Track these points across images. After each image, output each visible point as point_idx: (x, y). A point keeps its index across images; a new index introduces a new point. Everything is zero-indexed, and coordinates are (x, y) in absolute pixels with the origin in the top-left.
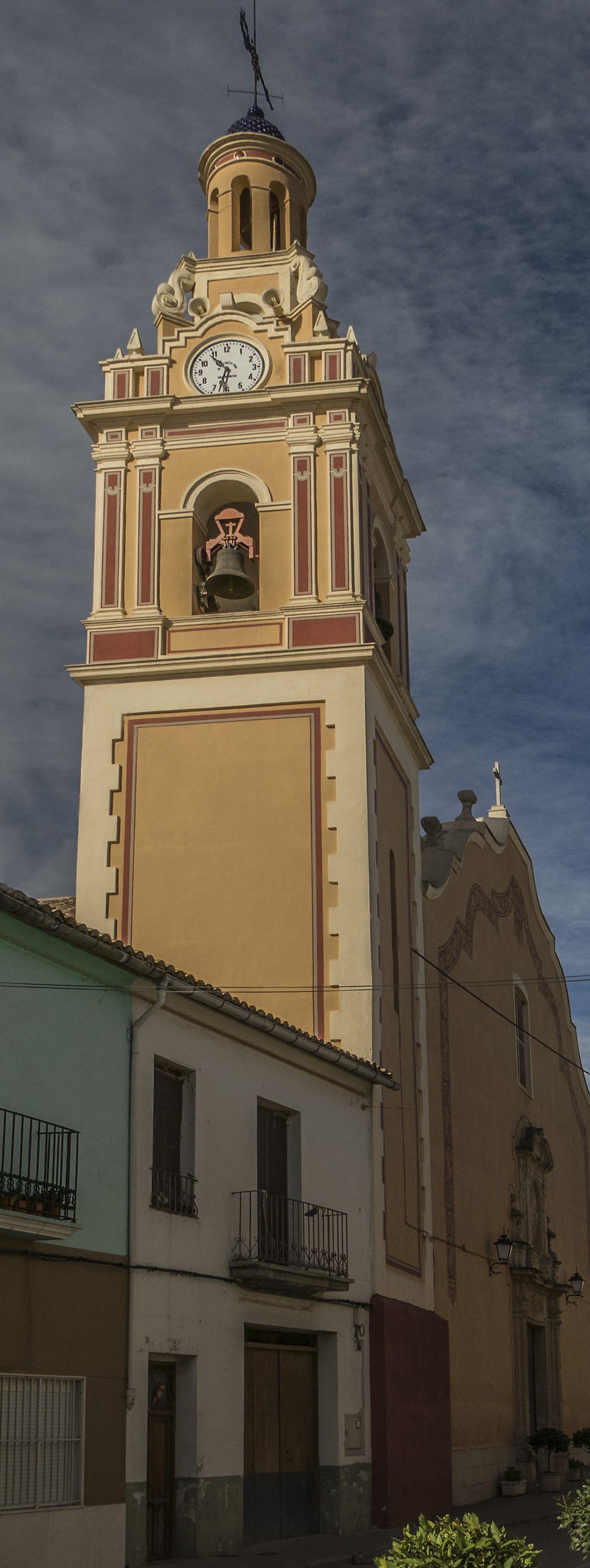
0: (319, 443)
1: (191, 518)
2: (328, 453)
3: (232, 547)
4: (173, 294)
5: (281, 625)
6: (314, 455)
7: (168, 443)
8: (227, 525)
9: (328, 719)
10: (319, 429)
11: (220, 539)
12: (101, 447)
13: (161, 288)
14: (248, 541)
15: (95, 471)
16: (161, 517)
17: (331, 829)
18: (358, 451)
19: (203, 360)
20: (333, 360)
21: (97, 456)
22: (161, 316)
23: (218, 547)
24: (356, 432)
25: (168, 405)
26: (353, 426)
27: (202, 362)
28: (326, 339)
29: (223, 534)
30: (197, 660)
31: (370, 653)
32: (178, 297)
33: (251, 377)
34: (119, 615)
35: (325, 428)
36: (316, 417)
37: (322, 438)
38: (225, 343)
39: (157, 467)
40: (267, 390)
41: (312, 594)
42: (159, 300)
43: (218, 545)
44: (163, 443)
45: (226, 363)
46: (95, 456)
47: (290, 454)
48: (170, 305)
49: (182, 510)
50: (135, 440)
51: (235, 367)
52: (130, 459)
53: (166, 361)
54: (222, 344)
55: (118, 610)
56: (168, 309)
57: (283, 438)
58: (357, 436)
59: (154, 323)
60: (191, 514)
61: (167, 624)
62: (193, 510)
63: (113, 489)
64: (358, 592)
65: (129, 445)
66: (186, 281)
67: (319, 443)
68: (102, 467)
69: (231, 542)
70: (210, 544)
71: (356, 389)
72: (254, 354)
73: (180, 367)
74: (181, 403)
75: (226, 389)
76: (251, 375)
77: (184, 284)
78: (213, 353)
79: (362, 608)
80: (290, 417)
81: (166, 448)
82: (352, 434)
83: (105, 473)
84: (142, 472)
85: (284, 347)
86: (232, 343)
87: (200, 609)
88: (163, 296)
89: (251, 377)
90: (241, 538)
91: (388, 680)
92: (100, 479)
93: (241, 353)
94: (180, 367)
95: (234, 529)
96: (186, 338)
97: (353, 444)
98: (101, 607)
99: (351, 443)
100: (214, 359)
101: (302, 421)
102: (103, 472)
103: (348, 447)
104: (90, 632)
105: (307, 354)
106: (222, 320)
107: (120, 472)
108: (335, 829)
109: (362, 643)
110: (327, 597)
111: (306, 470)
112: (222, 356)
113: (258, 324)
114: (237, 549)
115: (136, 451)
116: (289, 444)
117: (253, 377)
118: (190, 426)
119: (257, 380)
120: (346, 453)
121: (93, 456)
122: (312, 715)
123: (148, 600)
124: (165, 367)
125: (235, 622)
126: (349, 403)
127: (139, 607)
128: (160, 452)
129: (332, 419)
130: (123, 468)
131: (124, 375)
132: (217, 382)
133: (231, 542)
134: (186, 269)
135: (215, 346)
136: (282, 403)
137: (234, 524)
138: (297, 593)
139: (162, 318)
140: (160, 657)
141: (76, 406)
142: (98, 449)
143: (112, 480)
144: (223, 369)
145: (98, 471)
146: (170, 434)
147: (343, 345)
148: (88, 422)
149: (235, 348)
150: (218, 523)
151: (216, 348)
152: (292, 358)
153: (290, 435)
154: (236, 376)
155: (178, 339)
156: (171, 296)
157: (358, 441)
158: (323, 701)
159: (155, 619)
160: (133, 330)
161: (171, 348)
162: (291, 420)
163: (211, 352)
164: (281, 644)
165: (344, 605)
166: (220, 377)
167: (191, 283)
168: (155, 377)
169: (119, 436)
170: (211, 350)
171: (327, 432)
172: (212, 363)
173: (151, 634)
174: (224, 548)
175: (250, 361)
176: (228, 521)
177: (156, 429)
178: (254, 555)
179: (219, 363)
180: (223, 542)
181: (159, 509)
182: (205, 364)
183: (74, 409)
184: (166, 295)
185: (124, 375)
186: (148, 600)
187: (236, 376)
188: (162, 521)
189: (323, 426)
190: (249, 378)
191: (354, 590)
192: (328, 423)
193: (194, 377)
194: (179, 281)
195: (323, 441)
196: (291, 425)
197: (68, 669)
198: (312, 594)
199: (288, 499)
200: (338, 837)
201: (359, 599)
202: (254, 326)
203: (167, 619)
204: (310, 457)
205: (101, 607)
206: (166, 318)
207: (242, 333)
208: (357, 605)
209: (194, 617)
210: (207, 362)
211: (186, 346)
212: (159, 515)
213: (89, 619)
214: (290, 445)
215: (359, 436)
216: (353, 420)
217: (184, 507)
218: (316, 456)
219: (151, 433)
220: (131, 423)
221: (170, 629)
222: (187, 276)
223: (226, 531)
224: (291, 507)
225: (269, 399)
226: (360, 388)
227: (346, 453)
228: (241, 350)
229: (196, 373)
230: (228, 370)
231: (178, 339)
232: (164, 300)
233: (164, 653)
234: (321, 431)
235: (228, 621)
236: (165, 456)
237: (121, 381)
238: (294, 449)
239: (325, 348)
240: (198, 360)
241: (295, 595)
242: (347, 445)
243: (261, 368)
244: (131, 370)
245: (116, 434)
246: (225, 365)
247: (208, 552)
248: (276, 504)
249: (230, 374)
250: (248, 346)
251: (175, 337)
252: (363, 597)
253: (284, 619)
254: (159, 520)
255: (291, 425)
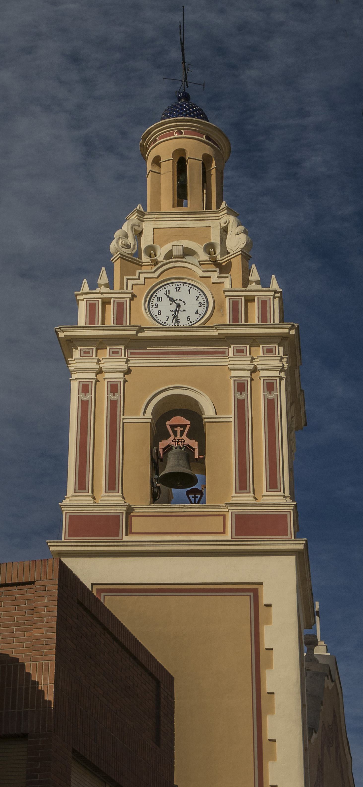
0: (255, 370)
1: (150, 423)
2: (262, 379)
3: (181, 448)
4: (127, 238)
5: (224, 516)
6: (250, 380)
7: (131, 361)
8: (175, 429)
9: (265, 599)
10: (254, 359)
11: (169, 441)
12: (76, 361)
13: (118, 234)
14: (194, 444)
15: (70, 380)
16: (125, 421)
17: (269, 693)
18: (286, 379)
19: (158, 296)
20: (264, 304)
21: (73, 368)
22: (119, 255)
23: (168, 448)
24: (284, 363)
25: (134, 333)
26: (282, 358)
27: (158, 298)
28: (260, 287)
29: (173, 437)
30: (158, 543)
31: (302, 547)
32: (131, 241)
33: (197, 312)
34: (89, 500)
35: (260, 358)
36: (251, 348)
37: (257, 366)
38: (177, 284)
39: (122, 380)
40: (216, 327)
41: (250, 493)
42: (117, 243)
43: (169, 446)
44: (127, 361)
45: (177, 300)
46: (71, 368)
47: (231, 377)
48: (126, 247)
49: (141, 416)
50: (105, 358)
51: (185, 304)
52: (100, 372)
53: (130, 295)
54: (174, 284)
55: (89, 496)
56: (124, 250)
57: (226, 364)
58: (286, 367)
59: (111, 260)
60: (150, 420)
61: (130, 510)
62: (152, 417)
63: (85, 395)
64: (287, 493)
65: (99, 360)
66: (136, 228)
67: (255, 370)
68: (77, 377)
69: (180, 443)
70: (163, 444)
71: (286, 331)
72: (200, 295)
73: (141, 301)
74: (144, 331)
75: (177, 321)
76: (197, 311)
77: (135, 230)
78: (166, 291)
79: (292, 508)
80: (230, 347)
81: (129, 365)
82: (282, 365)
83: (79, 382)
84: (110, 383)
85: (225, 291)
86: (182, 284)
87: (158, 499)
88: (121, 239)
89: (197, 312)
90: (188, 441)
91: (307, 564)
92: (75, 387)
93: (189, 293)
94: (141, 301)
95: (182, 433)
96: (145, 278)
97: (281, 372)
98: (75, 493)
99: (281, 371)
100: (168, 296)
101: (240, 351)
102: (78, 381)
103: (278, 375)
104: (66, 513)
105: (243, 298)
106: (174, 265)
107: (92, 382)
108: (273, 693)
109: (293, 538)
110: (263, 496)
111: (244, 391)
112: (174, 294)
113: (204, 271)
114: (184, 450)
115: (105, 365)
116: (230, 369)
117: (199, 313)
118: (148, 349)
119: (202, 315)
120: (277, 380)
121: (69, 368)
122: (252, 594)
123: (114, 489)
124: (128, 300)
125: (186, 512)
126: (279, 340)
127: (107, 494)
128: (125, 368)
129: (265, 351)
130: (94, 379)
131: (95, 304)
132: (171, 315)
133: (180, 443)
134: (137, 218)
135: (168, 286)
136: (226, 337)
137: (182, 429)
138: (238, 491)
139: (120, 257)
140: (125, 538)
141: (60, 328)
142: (74, 362)
143: (85, 388)
144: (174, 306)
145: (74, 379)
146: (132, 354)
147: (272, 293)
148: (67, 340)
149: (184, 288)
150: (168, 427)
151: (168, 288)
152: (231, 300)
153: (231, 363)
154: (185, 311)
155: (139, 279)
156: (125, 239)
157: (286, 370)
158: (262, 584)
159: (121, 505)
160: (101, 269)
161: (133, 285)
162: (231, 350)
163: (165, 290)
164: (224, 532)
165: (278, 504)
166: (172, 311)
167: (140, 229)
168: (120, 308)
169: (91, 353)
170: (165, 288)
171: (261, 362)
172: (166, 300)
173: (117, 518)
174: (173, 448)
175: (197, 300)
176: (176, 426)
177: (121, 349)
178: (199, 454)
179: (172, 300)
180: (173, 443)
181: (123, 415)
182: (160, 299)
183: (57, 330)
184: (123, 239)
185: (95, 304)
186: (114, 489)
187: (185, 311)
188: (125, 424)
189: (258, 357)
190: (196, 313)
191: (284, 492)
192: (261, 354)
193: (151, 309)
194: (132, 228)
195: (258, 368)
196: (231, 354)
197: (49, 544)
198: (250, 493)
199: (230, 413)
200: (275, 701)
201: (288, 499)
202: (201, 274)
203: (130, 506)
204: (247, 380)
205: (75, 493)
206: (123, 257)
207: (191, 278)
208: (289, 505)
209: (152, 505)
210: (161, 298)
211: (144, 284)
212: (123, 419)
213: (64, 502)
214: (230, 370)
215: (287, 367)
216: (281, 354)
217: (144, 414)
218: (252, 380)
219: (117, 352)
220: (101, 343)
221: (132, 514)
222: (137, 224)
223: (175, 433)
224: (232, 420)
225: (216, 333)
226: (290, 329)
227: (277, 380)
228: (189, 290)
229: (152, 306)
230: (179, 306)
231: (139, 279)
232: (122, 243)
233: (127, 535)
234: (256, 360)
235: (181, 510)
236: (128, 372)
237: (92, 308)
238: (234, 374)
239: (258, 294)
240: (154, 296)
241: (236, 493)
242: (277, 373)
243: (206, 306)
244: (100, 300)
245: (89, 350)
246: (177, 302)
247: (161, 451)
248: (218, 417)
249: (180, 309)
250: (195, 288)
251: (137, 277)
252: (292, 498)
253: (228, 512)
254: (123, 423)
255: (231, 354)
